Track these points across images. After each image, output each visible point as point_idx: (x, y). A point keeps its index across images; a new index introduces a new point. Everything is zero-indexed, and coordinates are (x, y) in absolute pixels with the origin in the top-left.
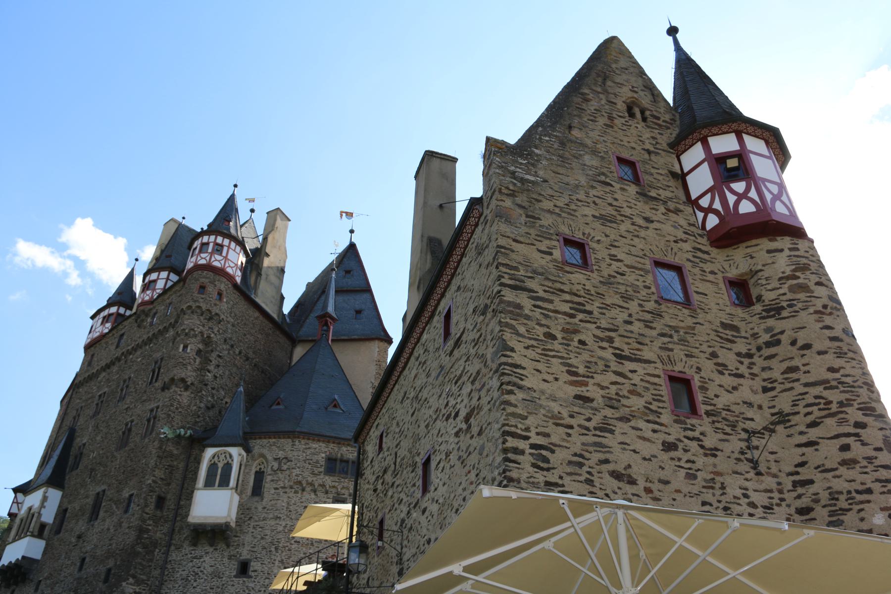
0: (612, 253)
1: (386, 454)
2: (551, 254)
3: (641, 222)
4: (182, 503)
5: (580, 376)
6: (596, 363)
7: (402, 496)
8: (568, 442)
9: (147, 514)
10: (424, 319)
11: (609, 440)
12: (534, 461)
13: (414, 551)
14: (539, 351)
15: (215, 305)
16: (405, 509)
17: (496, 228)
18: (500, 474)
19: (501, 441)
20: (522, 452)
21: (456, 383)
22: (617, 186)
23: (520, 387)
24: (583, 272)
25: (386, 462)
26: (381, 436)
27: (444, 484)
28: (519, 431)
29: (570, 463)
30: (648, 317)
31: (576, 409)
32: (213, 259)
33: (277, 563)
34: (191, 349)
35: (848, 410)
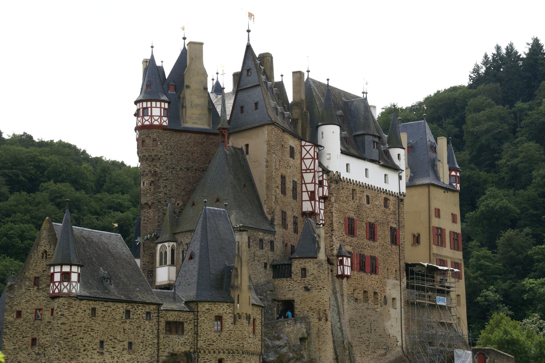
3: (35, 299)
11: (18, 356)
22: (32, 289)
23: (4, 349)
30: (31, 326)
32: (144, 120)
34: (146, 184)
35: (55, 344)
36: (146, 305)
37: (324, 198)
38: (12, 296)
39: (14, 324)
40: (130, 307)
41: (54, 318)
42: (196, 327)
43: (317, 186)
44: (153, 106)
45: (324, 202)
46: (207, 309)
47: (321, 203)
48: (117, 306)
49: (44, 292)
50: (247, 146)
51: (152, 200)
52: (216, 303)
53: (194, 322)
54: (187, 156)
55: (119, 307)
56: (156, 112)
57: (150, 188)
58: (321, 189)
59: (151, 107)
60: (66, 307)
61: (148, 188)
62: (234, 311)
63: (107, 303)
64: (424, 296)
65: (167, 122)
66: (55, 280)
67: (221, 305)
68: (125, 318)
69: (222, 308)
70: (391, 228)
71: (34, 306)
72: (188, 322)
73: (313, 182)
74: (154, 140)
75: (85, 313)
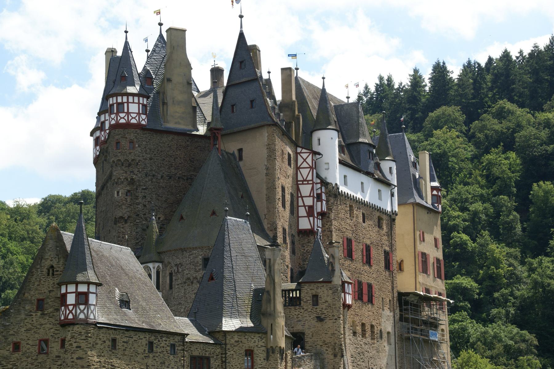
22: (34, 314)
30: (33, 361)
32: (119, 118)
34: (122, 193)
36: (170, 335)
37: (322, 215)
38: (8, 324)
39: (10, 360)
40: (153, 338)
41: (66, 351)
42: (224, 363)
43: (315, 200)
44: (129, 101)
45: (322, 219)
46: (236, 342)
47: (318, 220)
48: (139, 337)
49: (51, 319)
50: (240, 150)
51: (128, 213)
52: (247, 334)
53: (222, 357)
54: (169, 162)
55: (141, 337)
56: (134, 108)
57: (126, 199)
58: (319, 203)
59: (128, 102)
60: (83, 337)
61: (124, 199)
62: (267, 344)
63: (128, 333)
64: (416, 329)
65: (146, 120)
66: (68, 303)
67: (252, 337)
68: (149, 352)
69: (253, 340)
70: (385, 251)
71: (37, 336)
72: (215, 357)
73: (312, 195)
74: (131, 142)
75: (105, 344)
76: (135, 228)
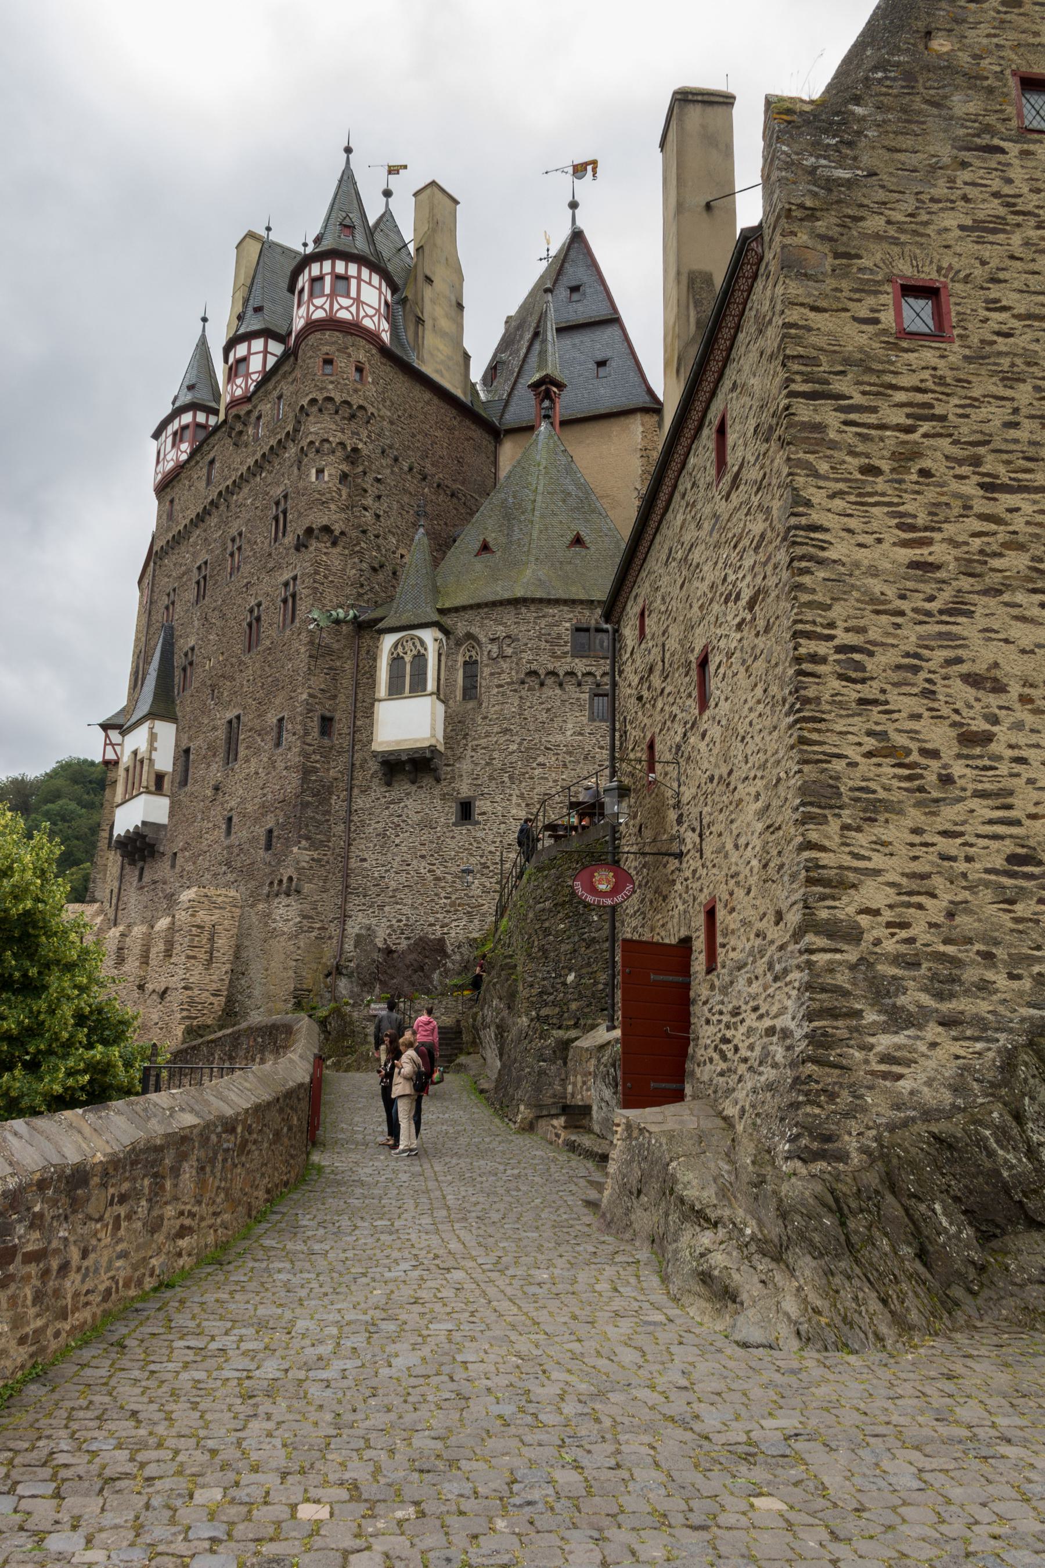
0: (992, 296)
1: (650, 644)
2: (876, 321)
4: (359, 723)
5: (920, 530)
6: (947, 504)
7: (675, 709)
8: (895, 636)
9: (310, 745)
10: (688, 433)
11: (964, 627)
12: (842, 671)
13: (693, 790)
14: (852, 498)
15: (356, 391)
16: (681, 731)
17: (781, 292)
18: (790, 693)
19: (792, 645)
20: (823, 660)
21: (735, 547)
22: (1013, 149)
23: (821, 562)
24: (933, 345)
25: (652, 657)
26: (642, 614)
27: (727, 699)
28: (819, 629)
29: (899, 667)
31: (910, 585)
32: (336, 307)
33: (514, 798)
34: (330, 475)
38: (844, 174)
39: (889, 378)
76: (356, 560)
